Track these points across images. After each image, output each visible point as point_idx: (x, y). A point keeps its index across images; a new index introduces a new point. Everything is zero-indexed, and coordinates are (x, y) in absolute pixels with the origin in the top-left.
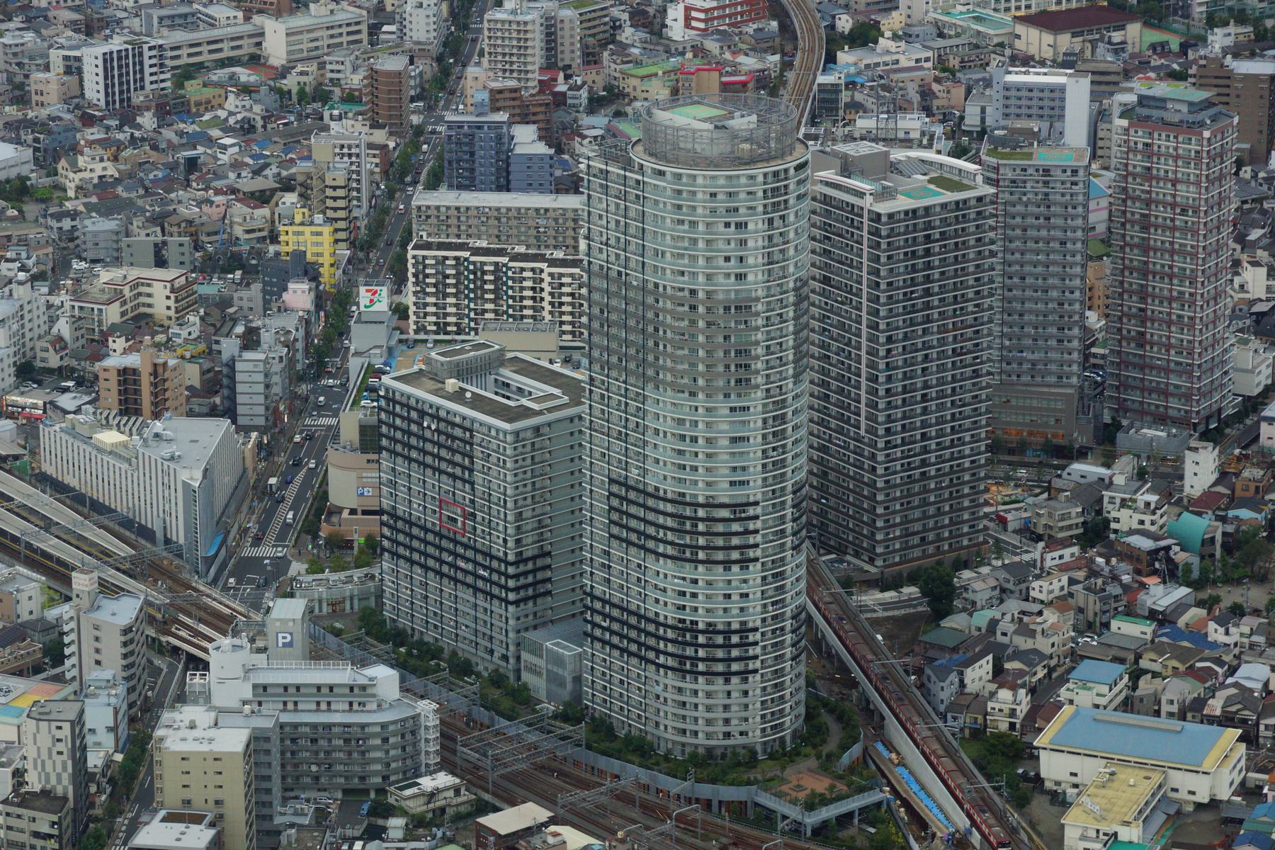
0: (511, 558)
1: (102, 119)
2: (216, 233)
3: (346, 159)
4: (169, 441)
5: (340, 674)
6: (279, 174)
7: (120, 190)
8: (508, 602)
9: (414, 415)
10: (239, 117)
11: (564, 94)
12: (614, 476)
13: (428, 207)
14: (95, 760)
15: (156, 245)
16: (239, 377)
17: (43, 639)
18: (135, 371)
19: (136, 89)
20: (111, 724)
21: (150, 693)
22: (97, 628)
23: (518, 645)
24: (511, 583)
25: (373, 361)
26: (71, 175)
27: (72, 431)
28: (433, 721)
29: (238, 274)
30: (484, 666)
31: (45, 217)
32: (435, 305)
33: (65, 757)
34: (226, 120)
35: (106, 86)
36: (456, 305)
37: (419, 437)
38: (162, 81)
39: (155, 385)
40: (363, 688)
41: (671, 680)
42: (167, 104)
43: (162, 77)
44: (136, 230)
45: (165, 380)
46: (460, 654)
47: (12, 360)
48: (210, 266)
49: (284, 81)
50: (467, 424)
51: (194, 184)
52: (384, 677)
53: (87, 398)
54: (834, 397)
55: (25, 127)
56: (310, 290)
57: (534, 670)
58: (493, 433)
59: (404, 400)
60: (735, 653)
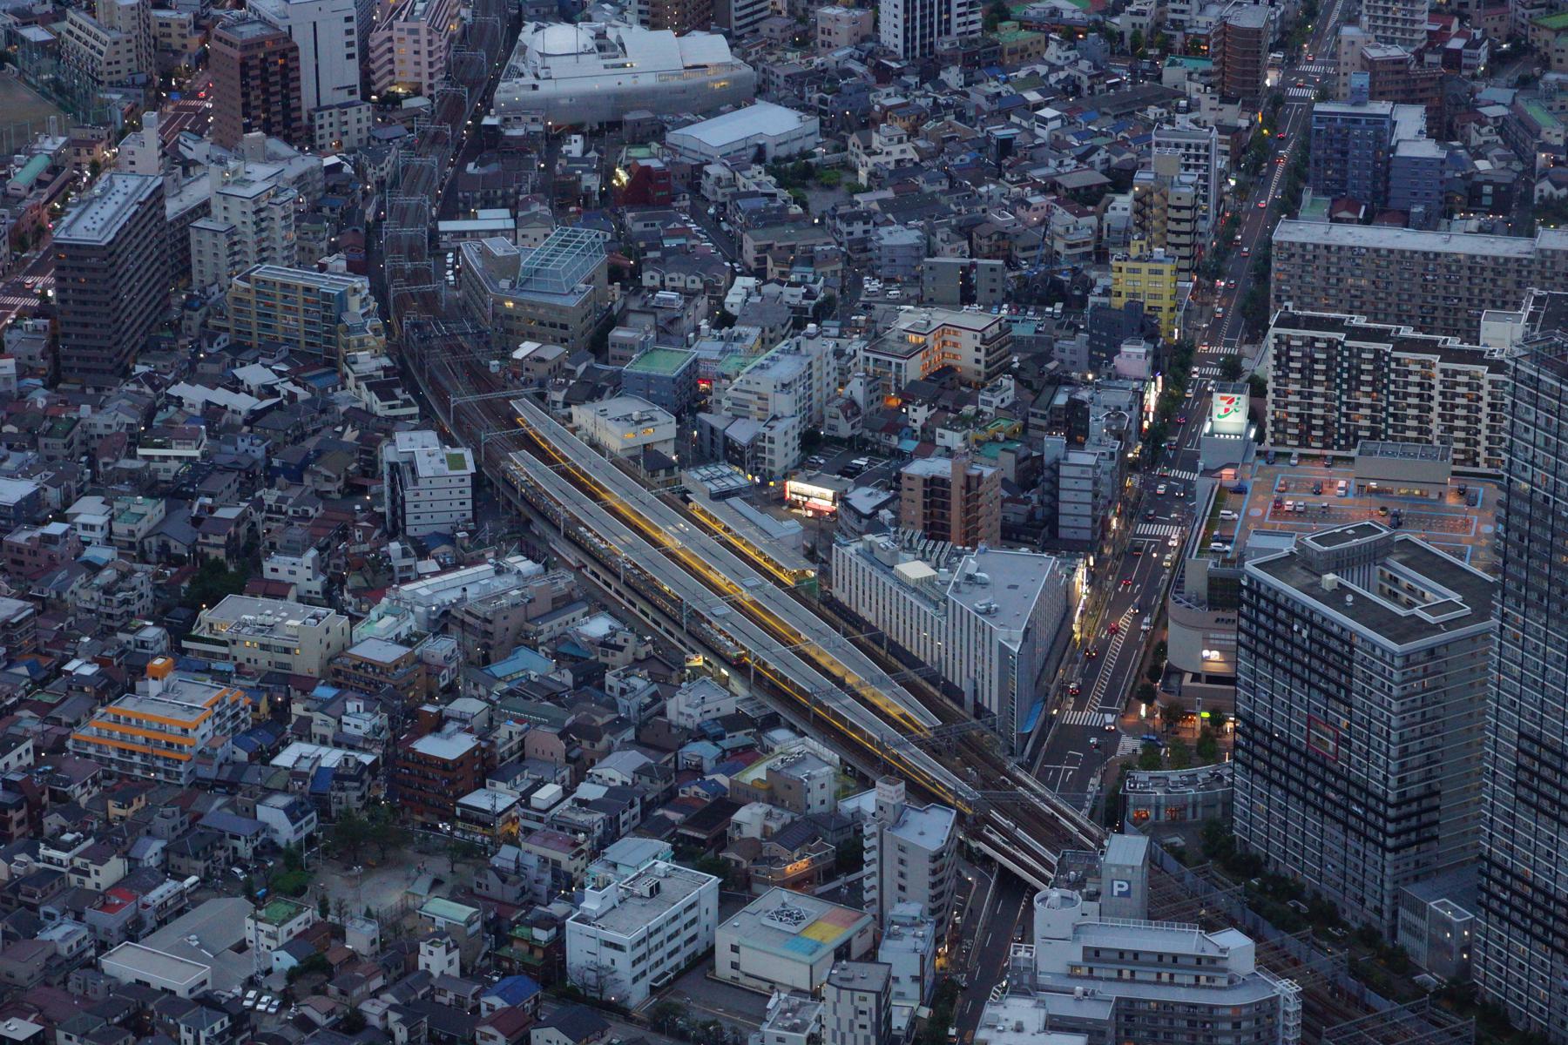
0: (1392, 797)
1: (900, 73)
2: (1032, 248)
3: (1192, 171)
4: (984, 584)
5: (1184, 941)
6: (1108, 160)
7: (920, 180)
8: (1385, 849)
9: (1281, 614)
10: (1062, 75)
11: (1458, 52)
12: (1525, 730)
13: (1292, 244)
14: (900, 1021)
16: (1063, 483)
18: (944, 482)
22: (902, 850)
23: (1395, 897)
24: (1391, 827)
26: (864, 158)
27: (869, 553)
28: (1294, 1007)
29: (1059, 305)
30: (1354, 917)
31: (833, 218)
32: (1299, 393)
33: (868, 1031)
34: (1046, 77)
35: (906, 30)
36: (1323, 395)
37: (1286, 641)
38: (972, 22)
40: (1213, 960)
42: (977, 52)
43: (972, 18)
46: (1325, 898)
47: (797, 431)
48: (1025, 296)
49: (1117, 20)
51: (1008, 176)
53: (884, 496)
55: (811, 83)
56: (1147, 353)
58: (1378, 652)
59: (1270, 595)
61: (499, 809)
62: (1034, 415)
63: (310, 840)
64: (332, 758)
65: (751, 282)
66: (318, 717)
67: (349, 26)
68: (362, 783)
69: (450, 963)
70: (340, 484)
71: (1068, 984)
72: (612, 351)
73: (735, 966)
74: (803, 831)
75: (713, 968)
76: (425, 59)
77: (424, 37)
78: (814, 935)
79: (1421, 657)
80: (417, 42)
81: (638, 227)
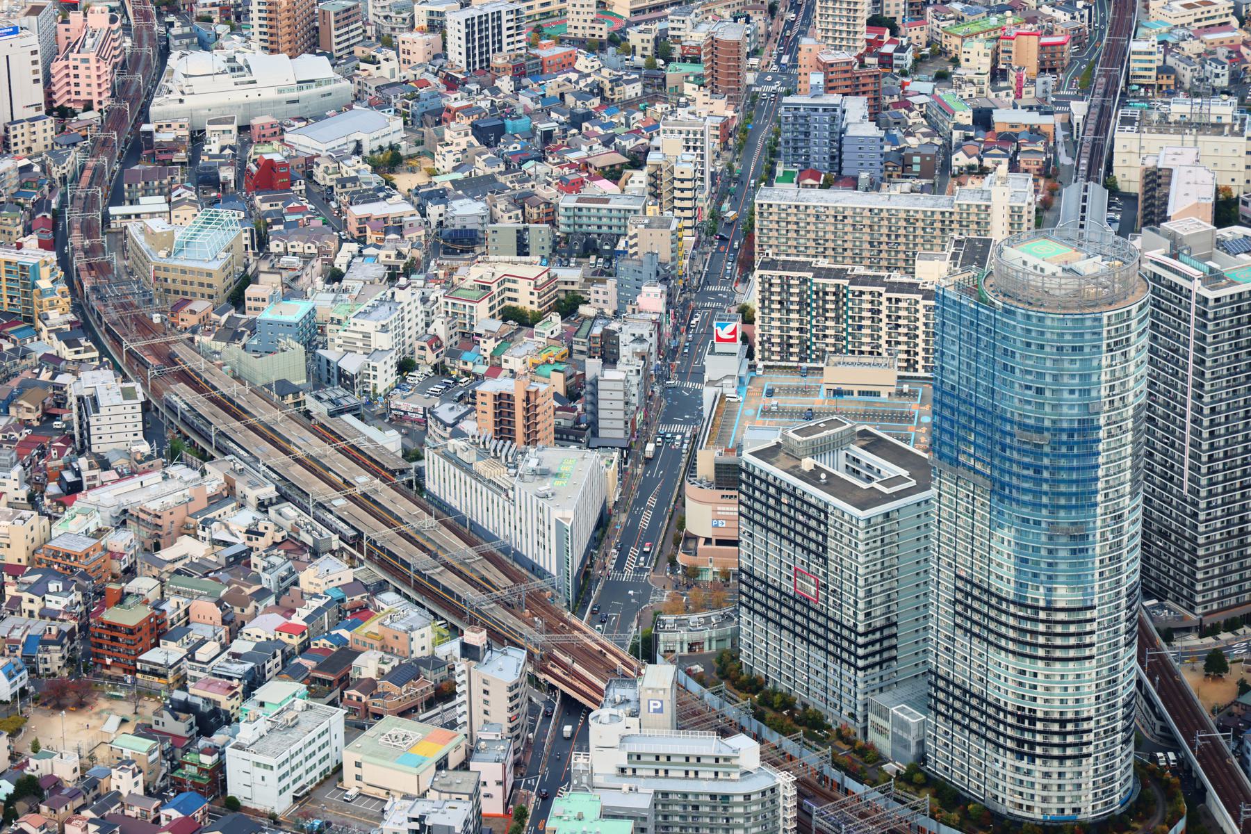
0: (861, 629)
1: (465, 82)
3: (691, 151)
5: (705, 744)
8: (857, 668)
9: (772, 490)
10: (589, 80)
11: (890, 55)
15: (518, 231)
17: (434, 677)
19: (494, 51)
20: (501, 779)
21: (531, 735)
22: (485, 682)
23: (866, 705)
24: (861, 652)
25: (726, 391)
28: (792, 792)
34: (577, 82)
35: (468, 49)
39: (527, 410)
41: (1010, 759)
43: (518, 38)
44: (500, 213)
45: (536, 407)
50: (821, 506)
51: (550, 159)
52: (745, 749)
54: (1158, 456)
57: (881, 731)
58: (846, 517)
59: (763, 476)
60: (1070, 739)
61: (171, 663)
62: (578, 343)
63: (23, 692)
64: (38, 627)
65: (355, 247)
66: (26, 596)
67: (35, 57)
68: (63, 646)
69: (136, 784)
70: (39, 413)
71: (616, 783)
72: (248, 303)
73: (358, 778)
74: (407, 672)
75: (341, 780)
76: (95, 82)
77: (93, 64)
78: (419, 752)
79: (880, 519)
80: (88, 68)
81: (266, 207)
